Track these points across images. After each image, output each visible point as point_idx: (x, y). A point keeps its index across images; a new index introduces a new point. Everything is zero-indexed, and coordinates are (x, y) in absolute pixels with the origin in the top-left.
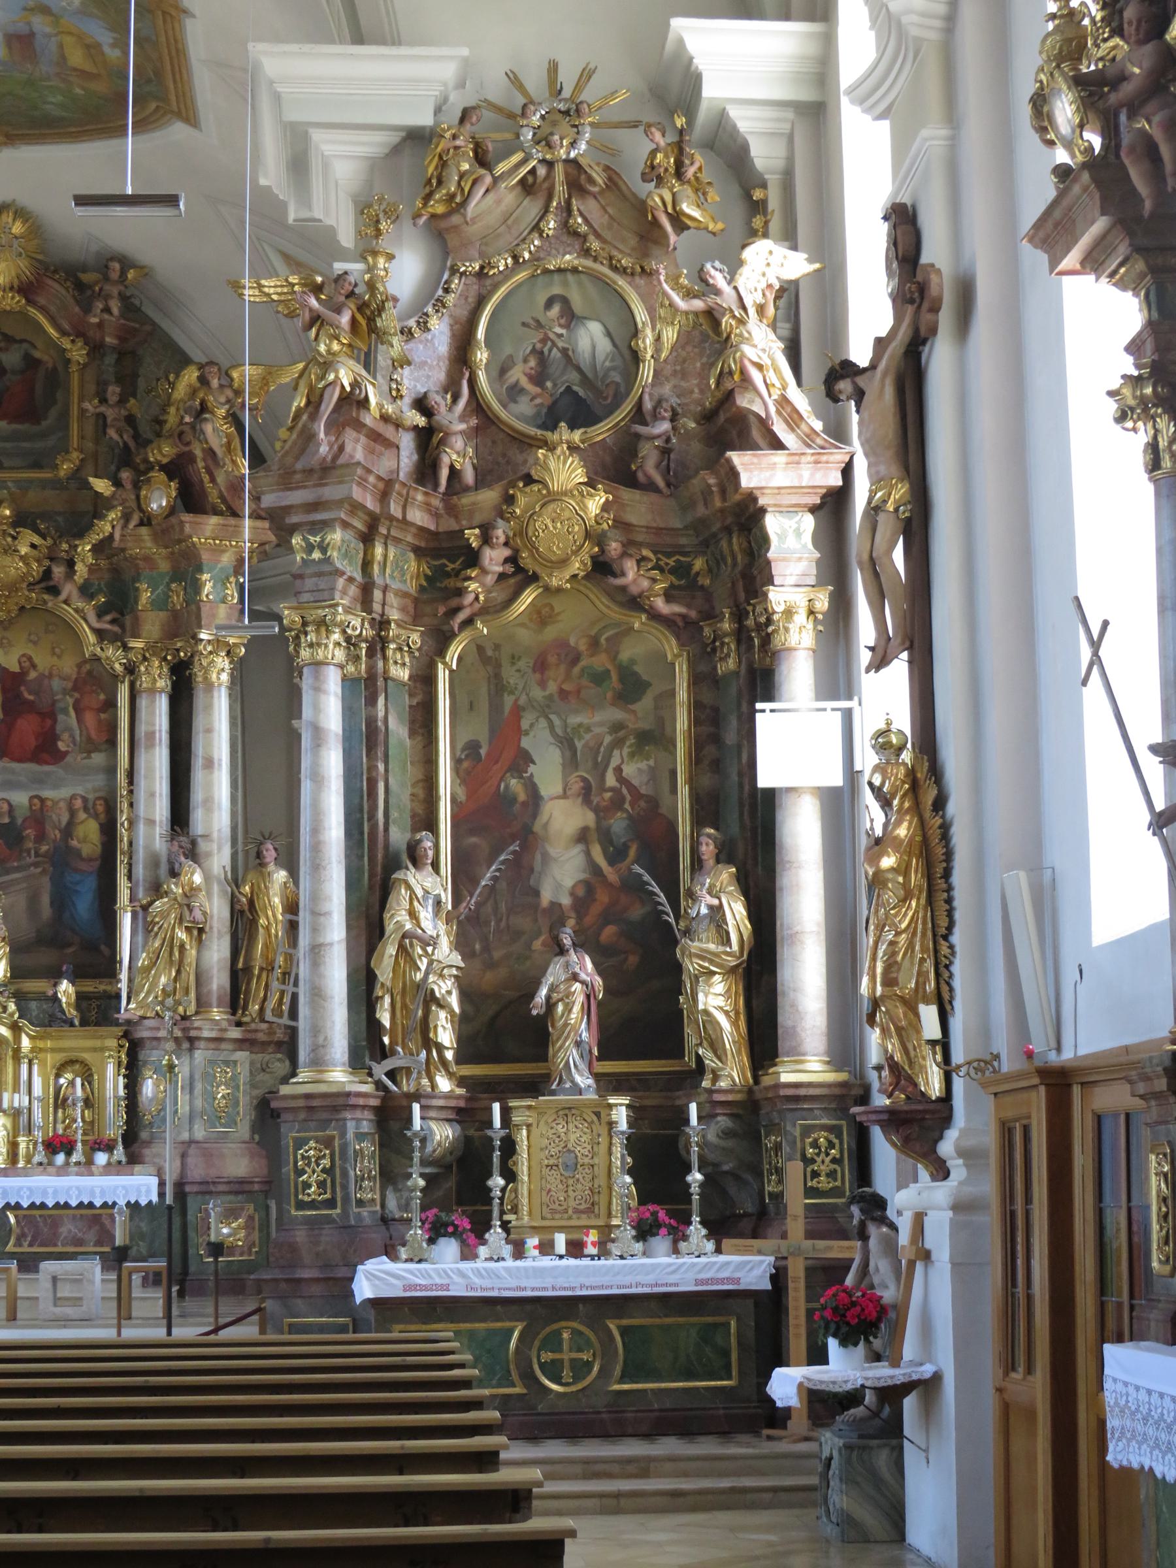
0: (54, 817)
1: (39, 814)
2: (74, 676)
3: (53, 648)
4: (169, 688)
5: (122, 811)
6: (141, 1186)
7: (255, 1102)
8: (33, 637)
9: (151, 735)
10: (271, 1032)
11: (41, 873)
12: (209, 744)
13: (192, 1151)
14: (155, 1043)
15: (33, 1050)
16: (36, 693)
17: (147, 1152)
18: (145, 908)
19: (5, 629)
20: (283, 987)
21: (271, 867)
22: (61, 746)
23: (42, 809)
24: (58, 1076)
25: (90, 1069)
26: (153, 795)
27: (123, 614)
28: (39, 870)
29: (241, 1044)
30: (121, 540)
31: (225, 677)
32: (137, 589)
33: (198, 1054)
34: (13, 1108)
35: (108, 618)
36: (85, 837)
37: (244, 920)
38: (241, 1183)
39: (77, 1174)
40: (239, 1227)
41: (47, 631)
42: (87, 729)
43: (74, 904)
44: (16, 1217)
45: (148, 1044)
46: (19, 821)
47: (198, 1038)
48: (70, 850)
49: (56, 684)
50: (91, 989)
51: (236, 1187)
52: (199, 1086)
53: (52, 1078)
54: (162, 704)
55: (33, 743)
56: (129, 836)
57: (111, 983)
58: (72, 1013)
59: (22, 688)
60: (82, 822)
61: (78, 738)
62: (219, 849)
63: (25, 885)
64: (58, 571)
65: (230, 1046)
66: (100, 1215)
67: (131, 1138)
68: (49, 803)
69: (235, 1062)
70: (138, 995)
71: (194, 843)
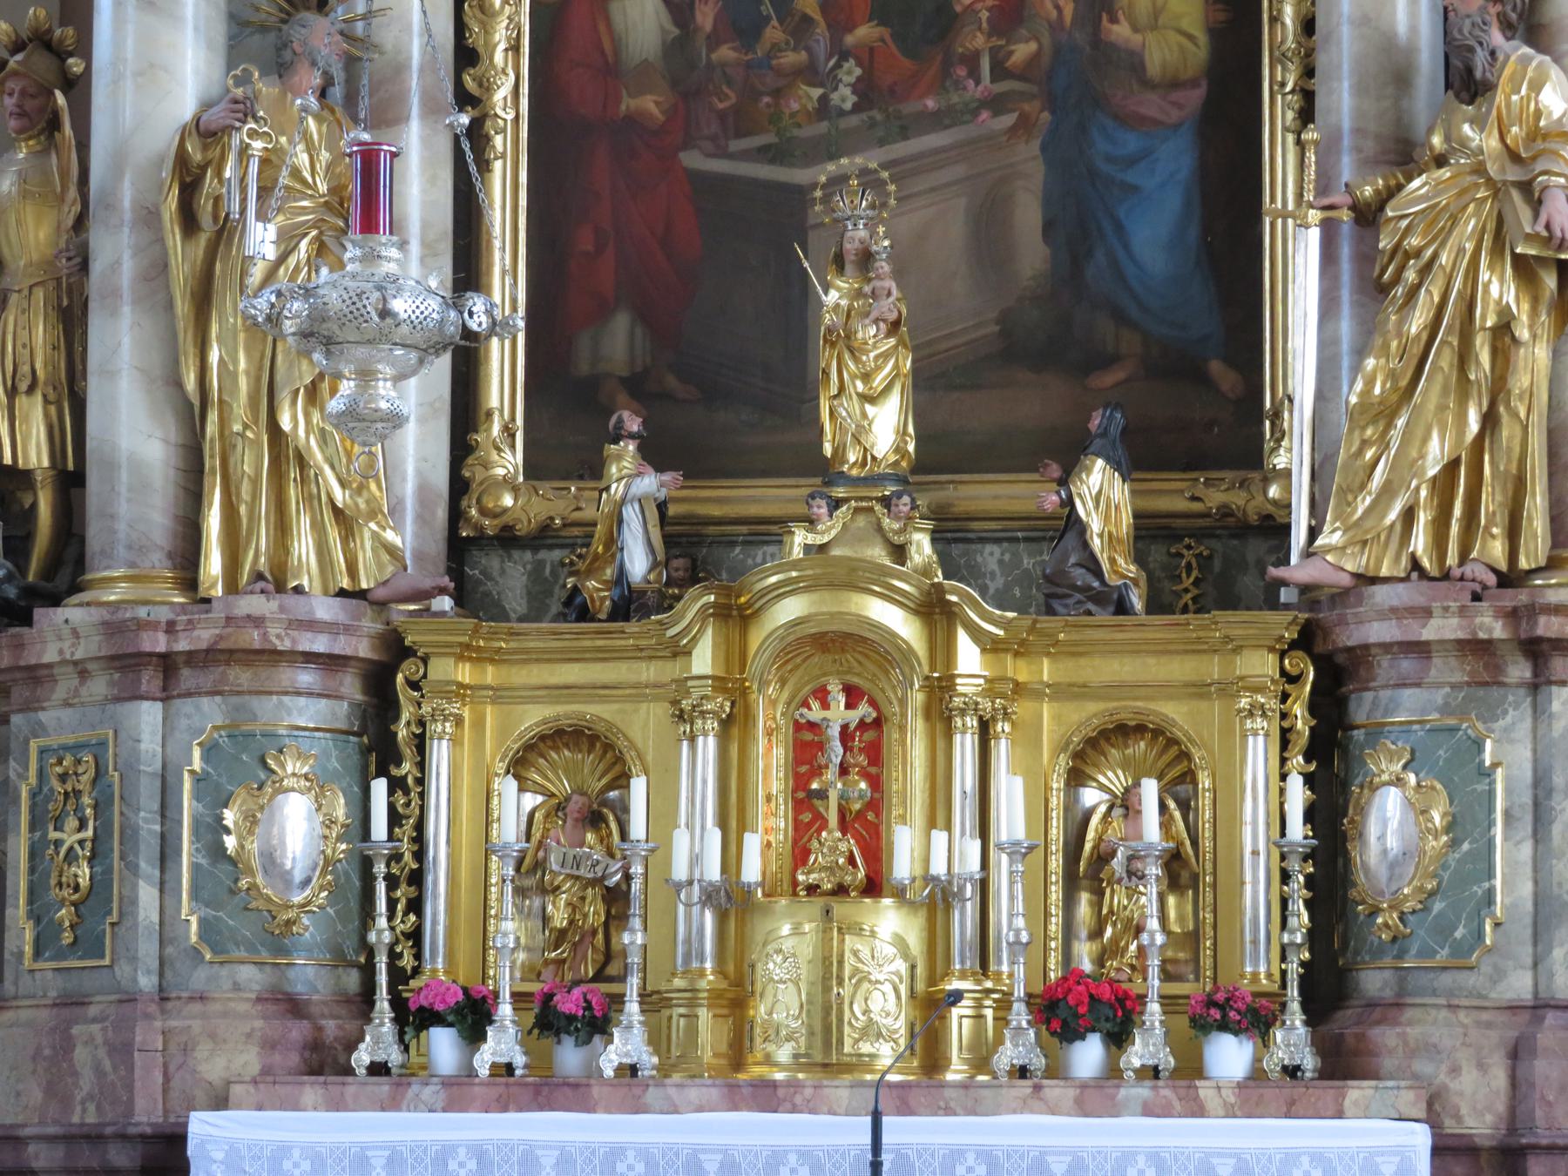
11: (1013, 131)
13: (1550, 1033)
14: (1407, 665)
15: (993, 686)
17: (1386, 1037)
18: (1368, 216)
24: (1077, 778)
25: (1185, 756)
28: (1008, 120)
34: (928, 879)
36: (1156, 13)
39: (1148, 1111)
43: (1119, 228)
45: (1385, 667)
48: (1104, 52)
50: (1181, 504)
53: (1057, 783)
58: (1121, 568)
63: (959, 171)
67: (1327, 988)
70: (1346, 503)
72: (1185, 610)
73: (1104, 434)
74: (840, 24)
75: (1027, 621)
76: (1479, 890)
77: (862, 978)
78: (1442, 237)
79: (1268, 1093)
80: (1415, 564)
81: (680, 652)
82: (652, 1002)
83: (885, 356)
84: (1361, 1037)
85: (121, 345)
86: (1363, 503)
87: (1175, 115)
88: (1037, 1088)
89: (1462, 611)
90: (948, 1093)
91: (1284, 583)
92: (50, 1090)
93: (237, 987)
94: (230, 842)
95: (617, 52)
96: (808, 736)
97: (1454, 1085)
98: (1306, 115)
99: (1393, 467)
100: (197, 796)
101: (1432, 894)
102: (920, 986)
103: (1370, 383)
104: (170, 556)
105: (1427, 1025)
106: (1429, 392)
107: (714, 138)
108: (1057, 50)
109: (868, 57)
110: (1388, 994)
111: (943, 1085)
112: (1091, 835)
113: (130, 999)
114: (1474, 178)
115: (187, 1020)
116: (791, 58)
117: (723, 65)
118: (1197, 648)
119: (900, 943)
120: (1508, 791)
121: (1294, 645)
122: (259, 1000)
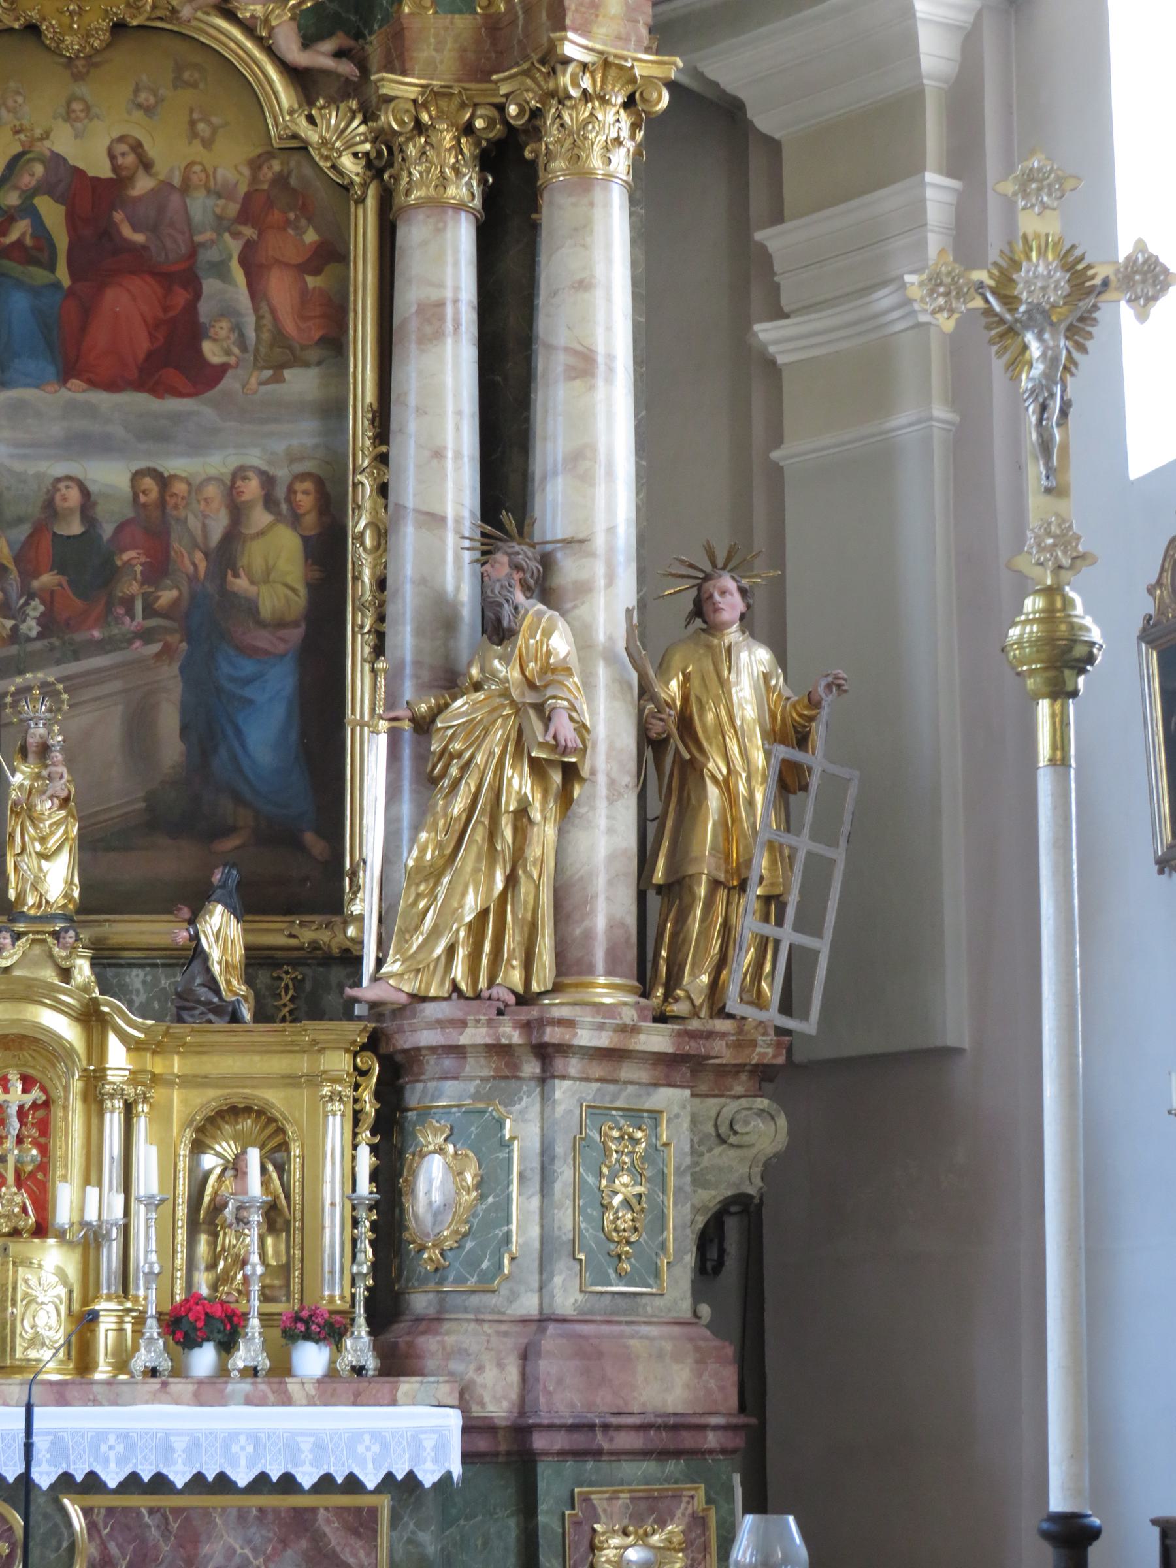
0: (193, 523)
2: (243, 189)
3: (192, 123)
4: (477, 203)
5: (358, 507)
6: (416, 1435)
7: (701, 1221)
8: (143, 97)
9: (433, 311)
10: (743, 1043)
11: (158, 656)
14: (448, 1063)
15: (135, 1077)
16: (154, 229)
17: (429, 1344)
18: (423, 726)
19: (78, 77)
20: (770, 930)
21: (733, 635)
22: (212, 352)
23: (162, 503)
24: (199, 1147)
25: (281, 1130)
27: (358, 35)
28: (156, 648)
29: (673, 1066)
31: (621, 162)
33: (562, 1090)
34: (83, 1224)
35: (328, 46)
36: (268, 571)
38: (676, 1428)
39: (249, 1401)
40: (669, 1547)
41: (178, 83)
42: (273, 311)
43: (238, 732)
44: (87, 1512)
45: (432, 1065)
46: (107, 530)
47: (564, 1049)
48: (228, 598)
49: (200, 207)
50: (281, 940)
51: (663, 1440)
52: (564, 1174)
53: (184, 1151)
55: (143, 345)
56: (374, 568)
58: (234, 988)
59: (118, 216)
60: (262, 533)
61: (251, 335)
63: (117, 685)
65: (642, 1074)
66: (314, 1510)
67: (386, 1307)
68: (180, 488)
69: (655, 1114)
70: (405, 940)
71: (547, 562)
72: (283, 1020)
73: (223, 886)
74: (28, 572)
75: (162, 1027)
76: (500, 1232)
77: (30, 1300)
78: (478, 743)
79: (340, 1387)
80: (455, 987)
83: (57, 824)
84: (410, 1344)
86: (417, 941)
87: (281, 647)
88: (165, 1384)
89: (490, 1022)
90: (96, 1388)
91: (356, 1000)
97: (479, 1380)
98: (379, 650)
99: (440, 914)
101: (465, 1235)
102: (76, 1307)
103: (423, 851)
105: (461, 1335)
106: (467, 858)
109: (49, 598)
110: (432, 1311)
111: (93, 1383)
112: (209, 1191)
114: (501, 700)
118: (288, 1049)
119: (61, 1273)
120: (522, 1158)
121: (364, 1048)
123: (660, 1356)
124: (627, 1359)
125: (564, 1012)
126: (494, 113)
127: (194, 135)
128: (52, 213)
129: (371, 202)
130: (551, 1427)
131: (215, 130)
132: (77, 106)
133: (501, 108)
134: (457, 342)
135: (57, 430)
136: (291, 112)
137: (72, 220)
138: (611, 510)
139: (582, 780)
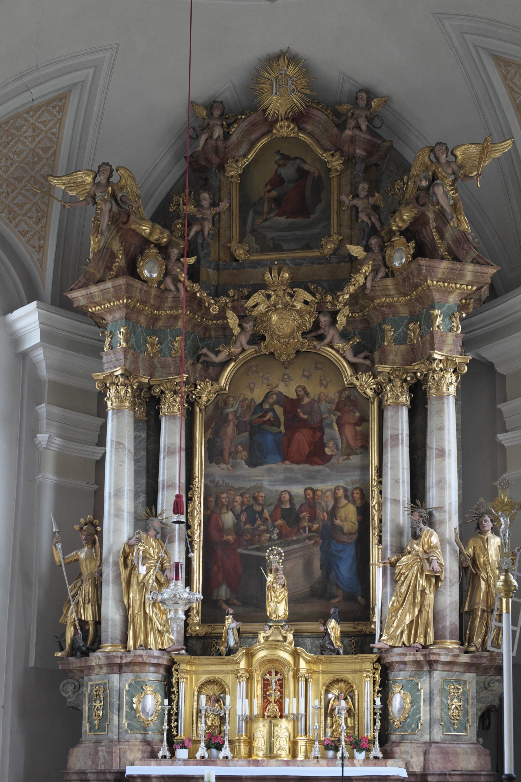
1: (311, 502)
2: (337, 400)
3: (321, 380)
4: (408, 403)
5: (373, 497)
9: (395, 438)
11: (313, 544)
12: (441, 439)
13: (433, 749)
14: (402, 666)
15: (308, 671)
16: (310, 414)
17: (397, 750)
18: (393, 565)
19: (286, 368)
21: (489, 534)
23: (314, 498)
24: (327, 692)
25: (352, 686)
26: (397, 481)
27: (372, 352)
28: (312, 542)
29: (469, 667)
30: (372, 290)
32: (383, 330)
35: (362, 355)
36: (346, 517)
37: (469, 573)
41: (317, 368)
42: (346, 438)
43: (338, 567)
46: (297, 507)
47: (436, 662)
48: (334, 527)
49: (323, 406)
52: (437, 699)
53: (323, 693)
54: (404, 414)
55: (307, 450)
56: (378, 515)
57: (365, 625)
58: (338, 644)
59: (299, 410)
60: (344, 506)
62: (450, 518)
63: (301, 553)
64: (324, 320)
67: (384, 739)
68: (319, 493)
69: (465, 682)
71: (430, 514)
72: (352, 654)
73: (334, 613)
74: (274, 521)
75: (316, 656)
78: (410, 569)
79: (370, 762)
80: (404, 643)
81: (237, 663)
82: (230, 742)
84: (391, 750)
85: (109, 592)
86: (392, 630)
87: (350, 541)
88: (318, 761)
91: (374, 648)
92: (93, 762)
93: (136, 739)
94: (135, 706)
95: (223, 526)
96: (266, 682)
97: (411, 760)
98: (380, 542)
99: (399, 622)
100: (127, 695)
101: (407, 718)
102: (292, 739)
104: (121, 641)
106: (407, 604)
107: (245, 546)
108: (324, 526)
109: (280, 527)
110: (397, 740)
111: (296, 761)
112: (330, 705)
113: (111, 741)
115: (124, 746)
116: (263, 528)
117: (247, 529)
120: (424, 694)
121: (376, 662)
122: (141, 742)
123: (467, 753)
124: (456, 754)
125: (436, 651)
126: (413, 375)
127: (321, 384)
128: (279, 410)
129: (376, 403)
130: (433, 774)
131: (328, 383)
132: (285, 377)
133: (415, 373)
134: (403, 447)
135: (281, 476)
136: (351, 376)
137: (285, 412)
138: (450, 498)
139: (441, 581)
